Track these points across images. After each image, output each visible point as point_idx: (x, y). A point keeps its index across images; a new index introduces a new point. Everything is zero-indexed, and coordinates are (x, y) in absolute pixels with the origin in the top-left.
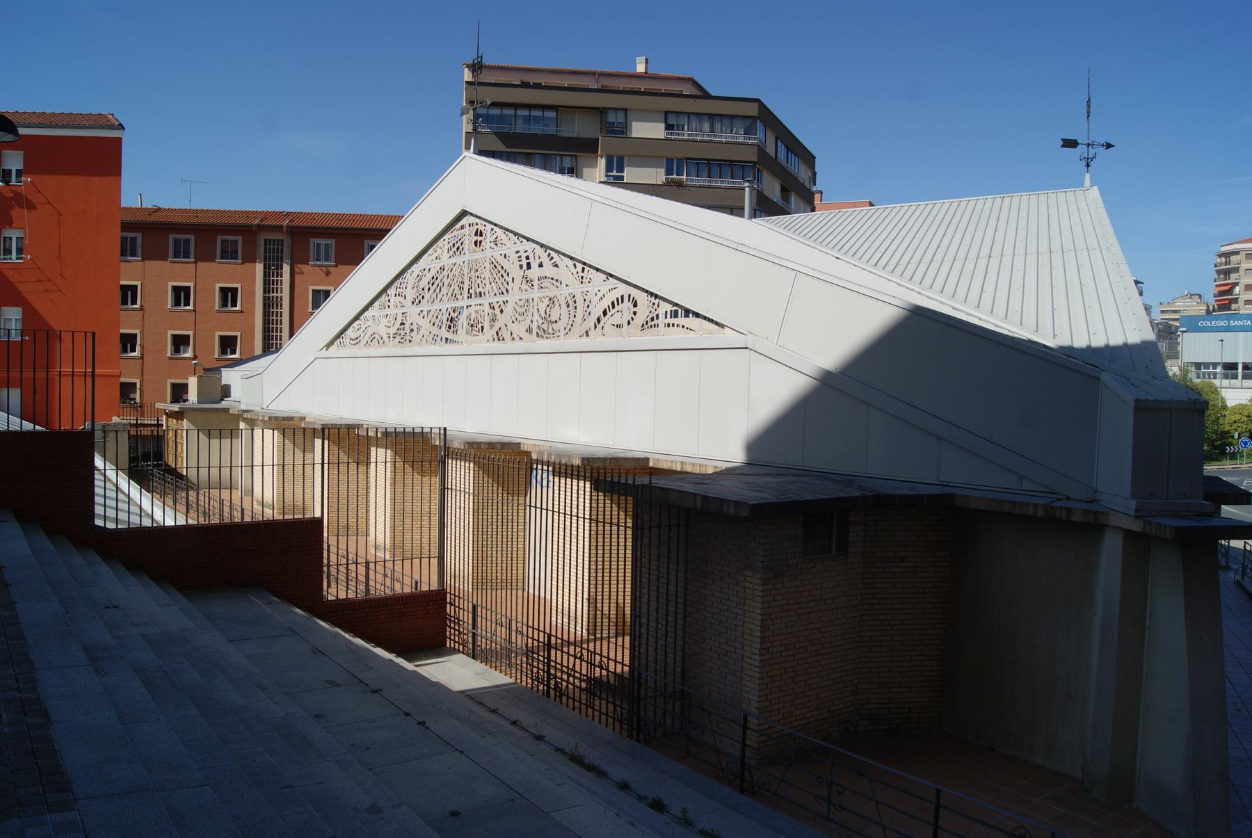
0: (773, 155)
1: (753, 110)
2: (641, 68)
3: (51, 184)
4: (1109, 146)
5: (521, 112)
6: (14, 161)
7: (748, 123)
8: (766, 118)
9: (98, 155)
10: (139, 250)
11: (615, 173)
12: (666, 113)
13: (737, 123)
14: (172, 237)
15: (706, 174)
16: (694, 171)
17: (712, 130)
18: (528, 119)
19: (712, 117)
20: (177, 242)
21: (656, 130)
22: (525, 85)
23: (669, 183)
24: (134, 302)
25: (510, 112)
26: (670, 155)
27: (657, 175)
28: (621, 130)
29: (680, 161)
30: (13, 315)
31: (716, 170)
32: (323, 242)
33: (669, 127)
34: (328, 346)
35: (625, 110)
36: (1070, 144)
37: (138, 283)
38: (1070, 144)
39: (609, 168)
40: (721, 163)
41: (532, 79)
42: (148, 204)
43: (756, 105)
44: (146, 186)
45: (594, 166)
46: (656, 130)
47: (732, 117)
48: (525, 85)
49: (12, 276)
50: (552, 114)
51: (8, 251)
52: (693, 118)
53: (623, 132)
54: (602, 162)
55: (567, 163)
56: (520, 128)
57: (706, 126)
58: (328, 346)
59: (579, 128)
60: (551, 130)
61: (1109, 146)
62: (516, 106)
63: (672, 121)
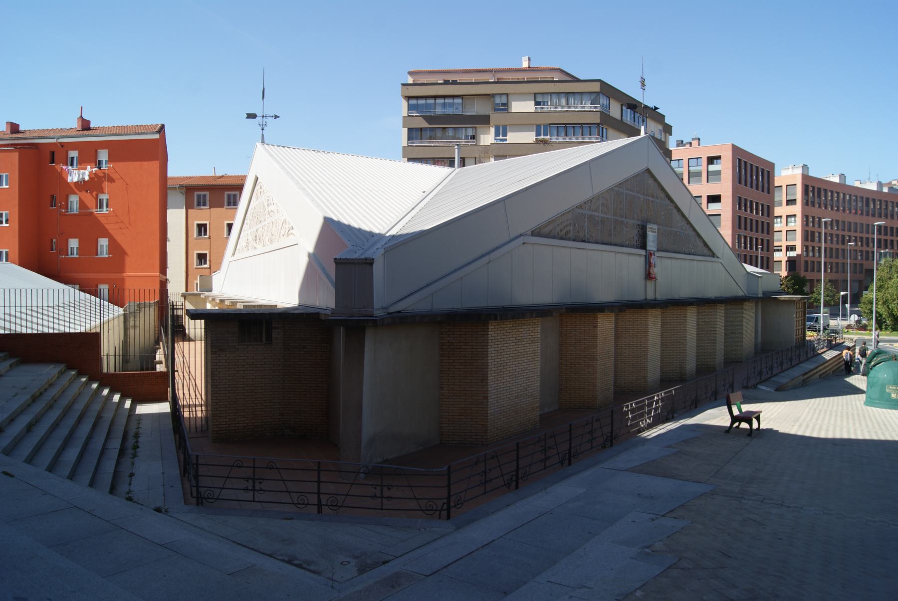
0: (619, 118)
1: (596, 87)
2: (525, 65)
3: (122, 166)
4: (276, 117)
5: (439, 101)
6: (103, 155)
7: (593, 97)
8: (608, 91)
9: (150, 148)
10: (208, 202)
11: (501, 137)
12: (535, 94)
13: (585, 97)
14: (226, 193)
15: (563, 133)
16: (555, 132)
17: (567, 103)
18: (444, 105)
19: (567, 94)
20: (229, 196)
21: (528, 106)
22: (446, 83)
23: (538, 142)
24: (205, 234)
25: (431, 101)
26: (538, 123)
27: (529, 137)
28: (506, 107)
29: (545, 126)
30: (104, 242)
31: (570, 130)
32: (202, 193)
33: (537, 104)
34: (233, 254)
35: (507, 95)
36: (251, 116)
37: (207, 222)
38: (251, 116)
39: (497, 134)
40: (574, 126)
41: (451, 78)
42: (219, 174)
43: (599, 84)
44: (181, 166)
45: (488, 133)
46: (528, 106)
47: (581, 93)
48: (446, 83)
49: (103, 221)
50: (459, 101)
51: (101, 207)
52: (554, 97)
53: (505, 110)
54: (492, 130)
55: (470, 132)
56: (439, 111)
57: (563, 101)
58: (233, 254)
59: (477, 109)
60: (459, 111)
61: (276, 117)
62: (435, 97)
63: (539, 99)
